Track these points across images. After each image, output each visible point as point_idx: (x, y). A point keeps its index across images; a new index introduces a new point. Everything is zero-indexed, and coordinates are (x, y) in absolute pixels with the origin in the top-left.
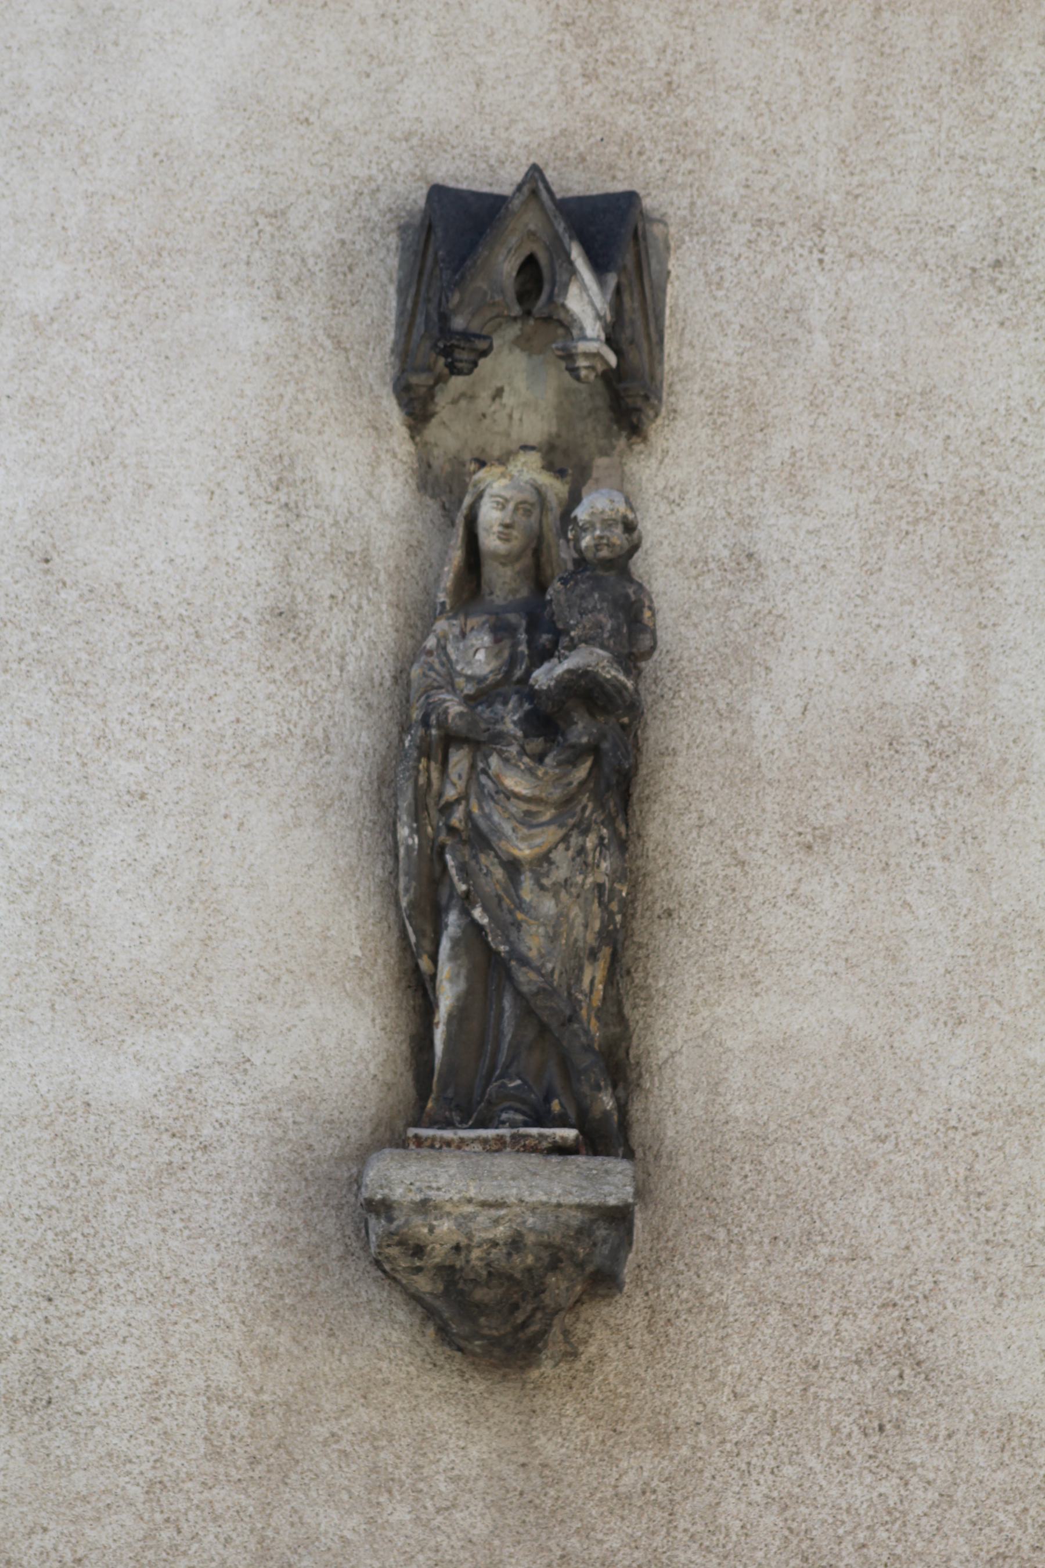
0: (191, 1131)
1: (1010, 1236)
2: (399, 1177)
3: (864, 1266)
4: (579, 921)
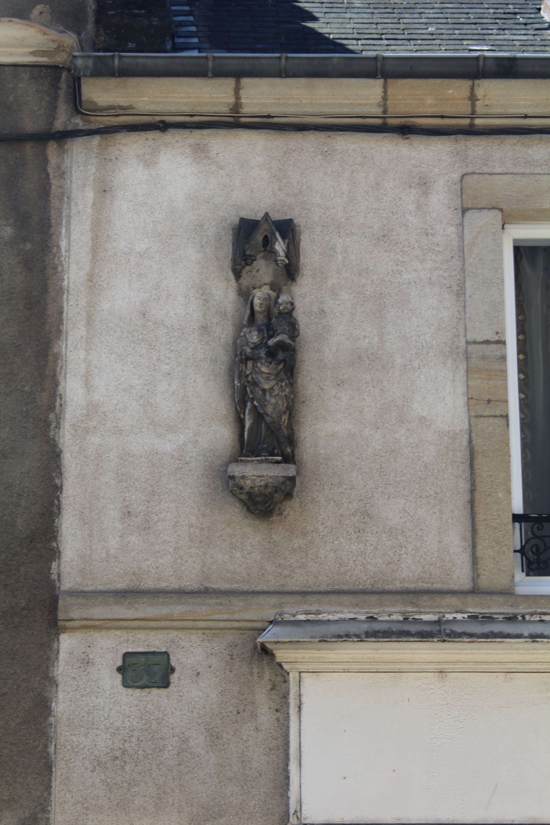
0: (183, 459)
2: (236, 470)
3: (354, 490)
4: (281, 404)
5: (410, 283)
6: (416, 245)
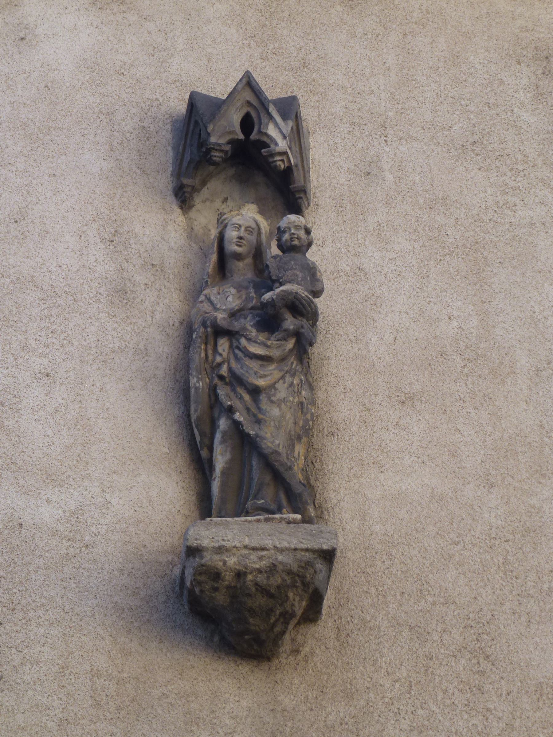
0: (79, 538)
1: (531, 592)
3: (453, 607)
4: (291, 421)
5: (532, 225)
6: (540, 162)
